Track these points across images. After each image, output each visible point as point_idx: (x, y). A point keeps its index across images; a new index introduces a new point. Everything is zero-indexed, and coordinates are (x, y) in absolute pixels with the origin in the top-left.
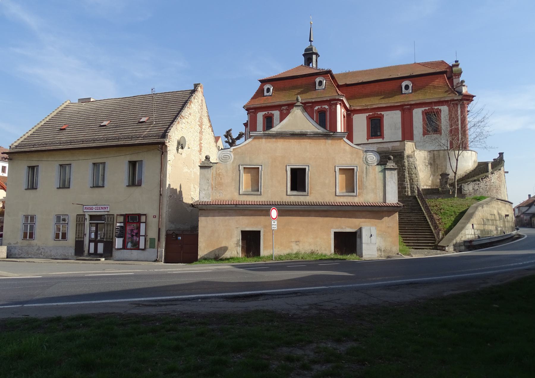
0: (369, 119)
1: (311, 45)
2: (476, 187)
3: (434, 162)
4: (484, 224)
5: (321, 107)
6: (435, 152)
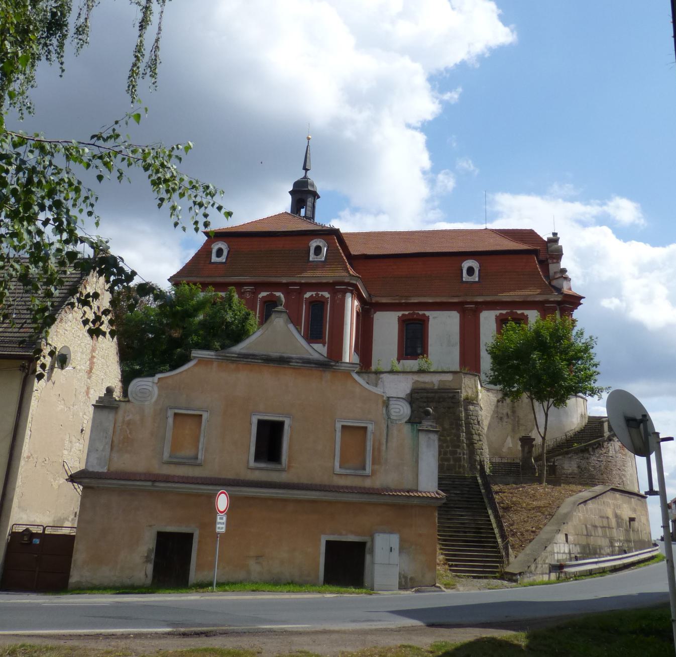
0: (403, 321)
1: (305, 177)
4: (587, 535)
5: (317, 295)
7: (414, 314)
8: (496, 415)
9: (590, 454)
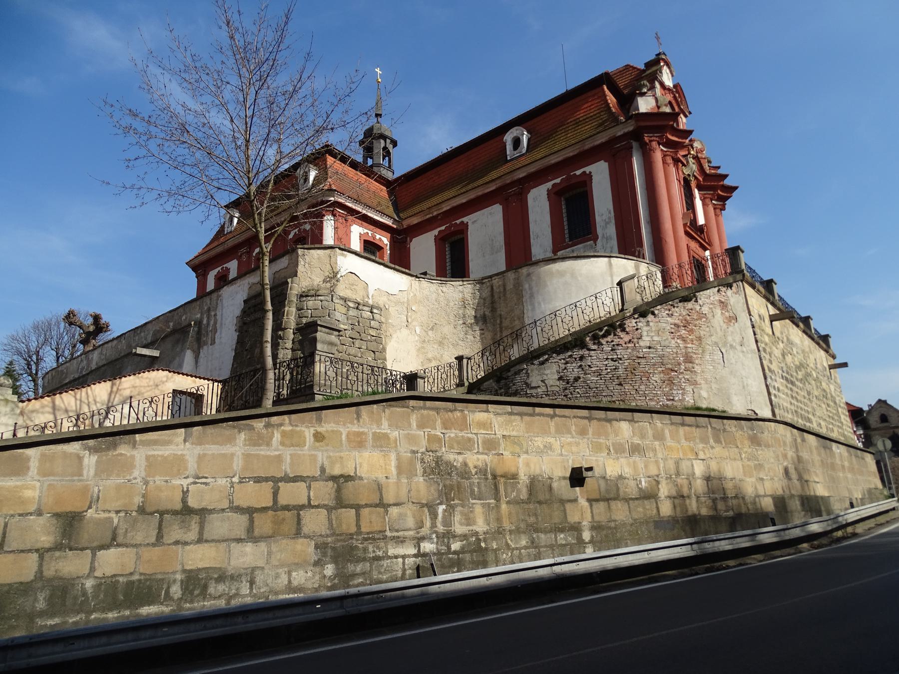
2: (573, 370)
3: (493, 310)
6: (496, 282)
7: (450, 227)
8: (461, 322)
9: (589, 350)
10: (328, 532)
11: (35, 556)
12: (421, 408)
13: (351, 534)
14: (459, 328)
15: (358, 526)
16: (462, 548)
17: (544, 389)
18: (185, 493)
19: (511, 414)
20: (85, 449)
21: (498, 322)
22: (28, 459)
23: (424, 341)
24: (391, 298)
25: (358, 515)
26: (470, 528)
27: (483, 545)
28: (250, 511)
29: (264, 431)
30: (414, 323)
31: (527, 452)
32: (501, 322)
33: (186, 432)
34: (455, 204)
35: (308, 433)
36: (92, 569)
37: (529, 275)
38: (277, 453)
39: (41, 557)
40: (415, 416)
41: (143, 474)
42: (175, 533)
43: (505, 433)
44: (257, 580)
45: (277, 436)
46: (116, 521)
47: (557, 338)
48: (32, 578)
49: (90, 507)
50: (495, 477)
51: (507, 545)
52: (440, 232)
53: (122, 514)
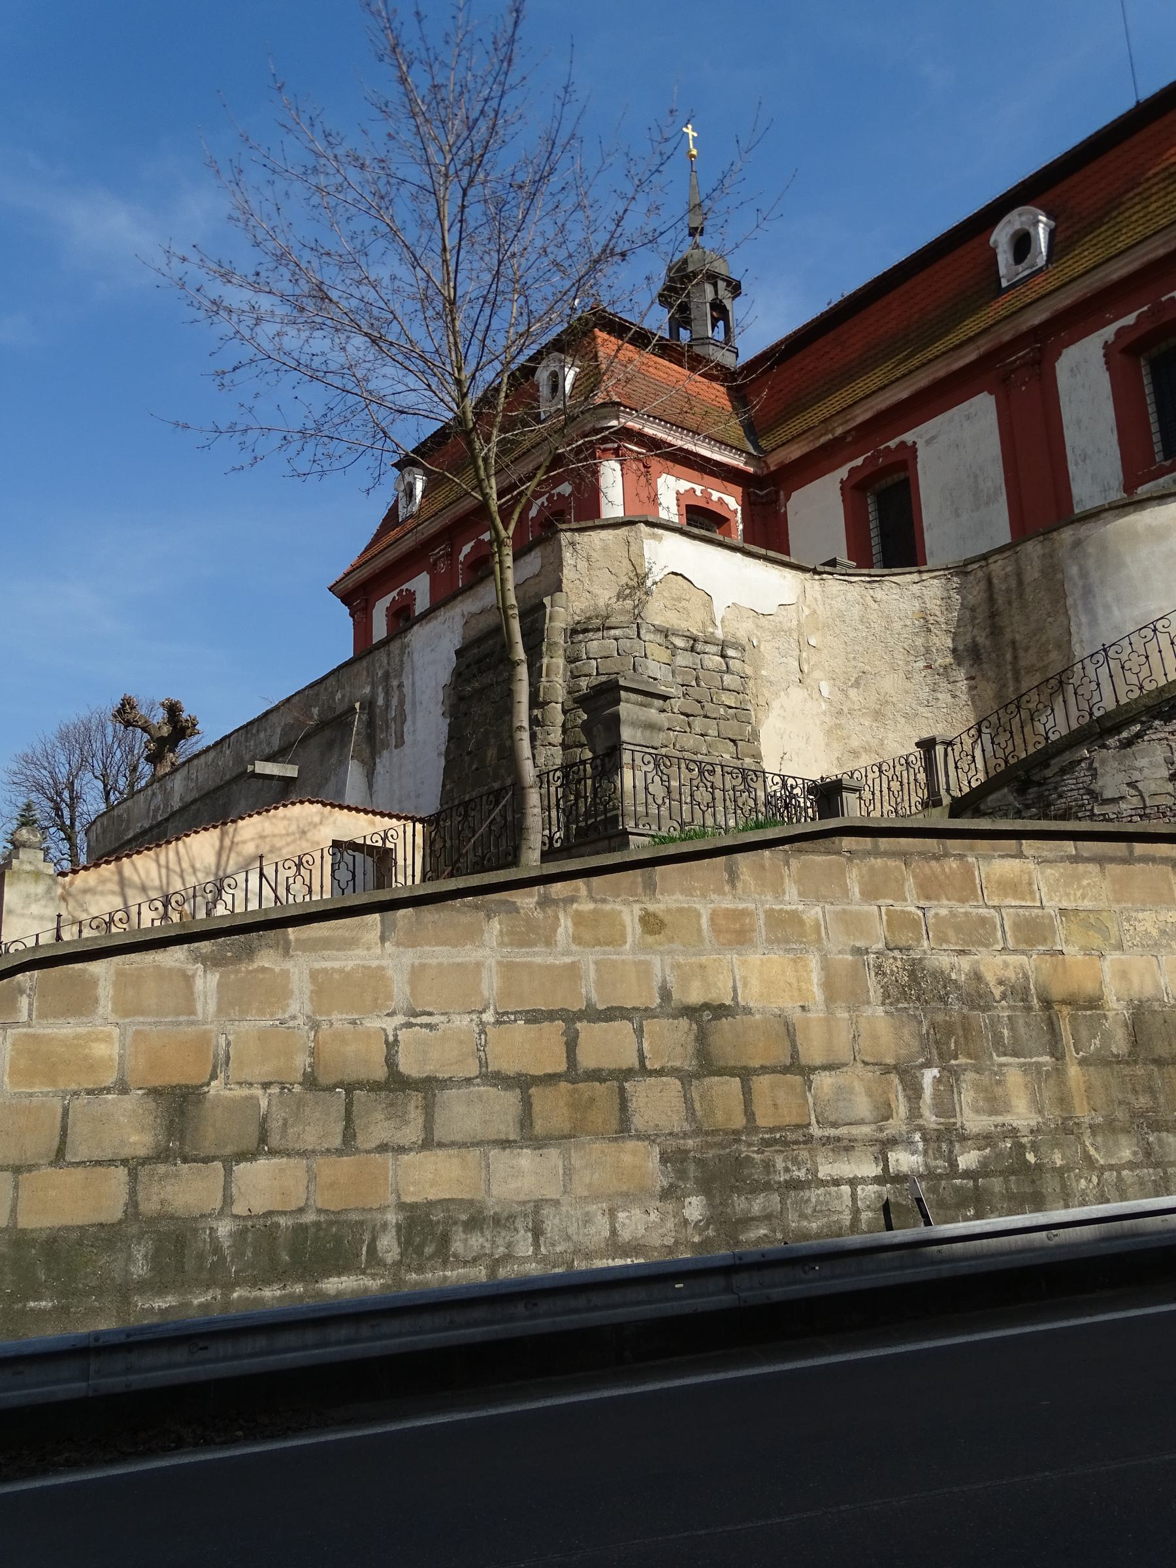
3: (995, 631)
7: (874, 458)
8: (921, 664)
10: (687, 1127)
11: (121, 1173)
12: (868, 854)
13: (736, 1132)
14: (918, 677)
15: (749, 1114)
16: (984, 1163)
17: (1136, 802)
18: (392, 1046)
19: (1076, 859)
20: (195, 960)
21: (1009, 657)
22: (94, 982)
23: (840, 712)
24: (763, 621)
25: (747, 1091)
26: (1000, 1119)
27: (1031, 1158)
28: (523, 1083)
29: (539, 914)
30: (817, 674)
31: (1120, 947)
32: (1015, 658)
33: (382, 921)
34: (883, 406)
35: (629, 916)
36: (228, 1200)
37: (1077, 543)
38: (568, 960)
39: (133, 1176)
40: (855, 872)
41: (308, 1008)
42: (377, 1128)
43: (1064, 904)
44: (548, 1226)
45: (565, 925)
46: (264, 1103)
47: (1162, 682)
48: (119, 1215)
49: (214, 1076)
50: (1047, 1004)
51: (1088, 1158)
52: (851, 471)
53: (275, 1090)
